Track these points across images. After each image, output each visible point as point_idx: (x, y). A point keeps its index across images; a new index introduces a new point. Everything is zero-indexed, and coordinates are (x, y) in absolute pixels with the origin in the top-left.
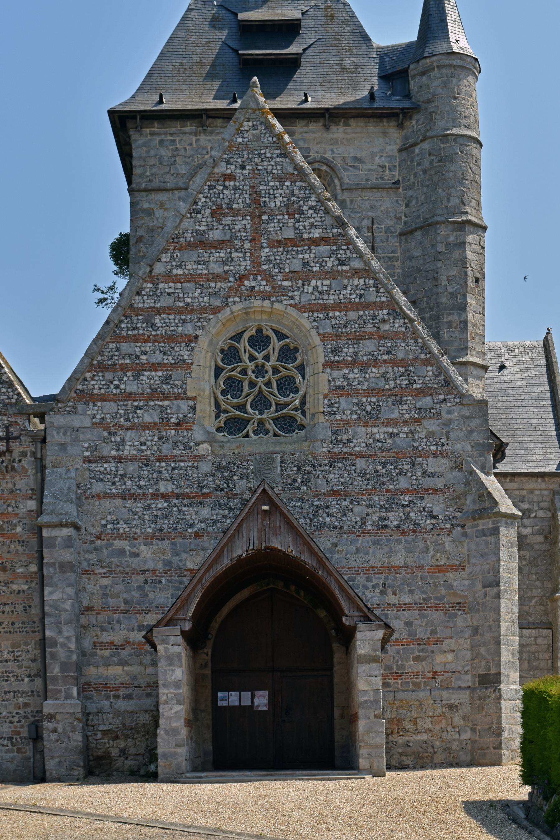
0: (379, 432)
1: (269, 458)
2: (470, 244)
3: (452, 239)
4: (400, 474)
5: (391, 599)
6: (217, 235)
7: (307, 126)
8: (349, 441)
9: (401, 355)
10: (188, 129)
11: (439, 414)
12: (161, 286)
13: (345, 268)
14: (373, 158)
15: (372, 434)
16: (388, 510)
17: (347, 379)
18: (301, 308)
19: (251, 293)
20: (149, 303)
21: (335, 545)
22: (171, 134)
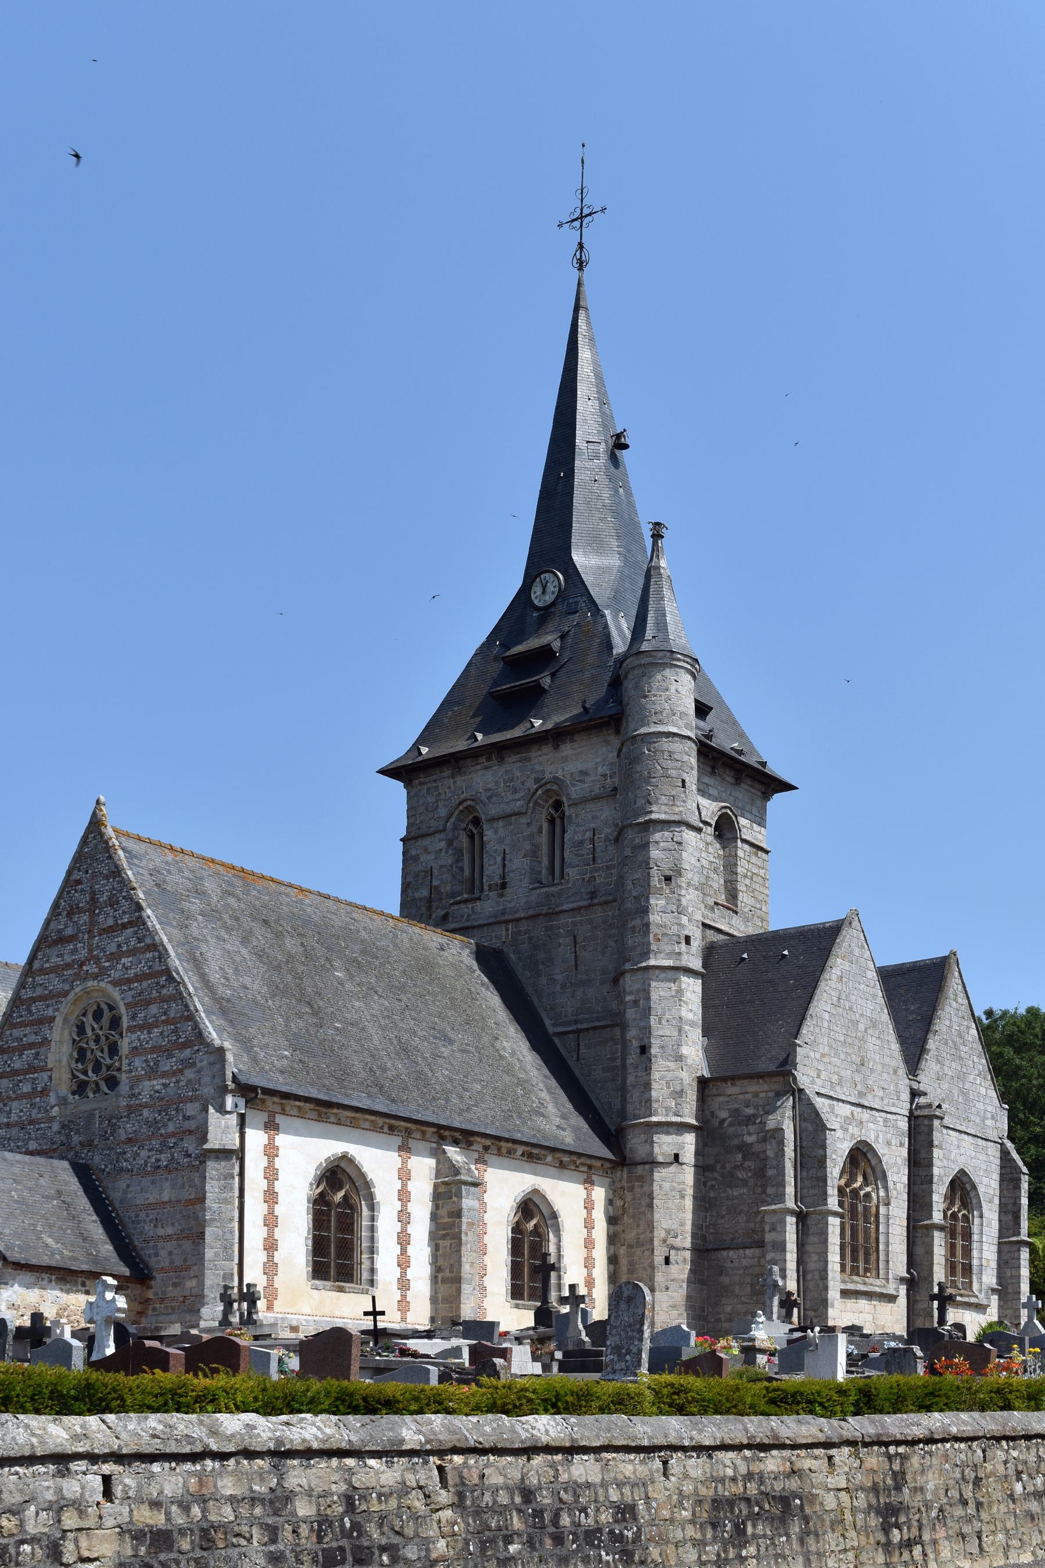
0: (157, 1084)
1: (90, 1115)
2: (657, 842)
3: (637, 841)
4: (169, 1120)
5: (161, 1232)
6: (69, 931)
7: (539, 749)
8: (140, 1094)
9: (172, 1014)
10: (446, 774)
11: (194, 1063)
12: (37, 978)
13: (142, 945)
14: (596, 768)
15: (154, 1086)
16: (161, 1152)
17: (139, 1040)
18: (115, 983)
19: (88, 977)
20: (30, 994)
21: (128, 1186)
22: (435, 781)
